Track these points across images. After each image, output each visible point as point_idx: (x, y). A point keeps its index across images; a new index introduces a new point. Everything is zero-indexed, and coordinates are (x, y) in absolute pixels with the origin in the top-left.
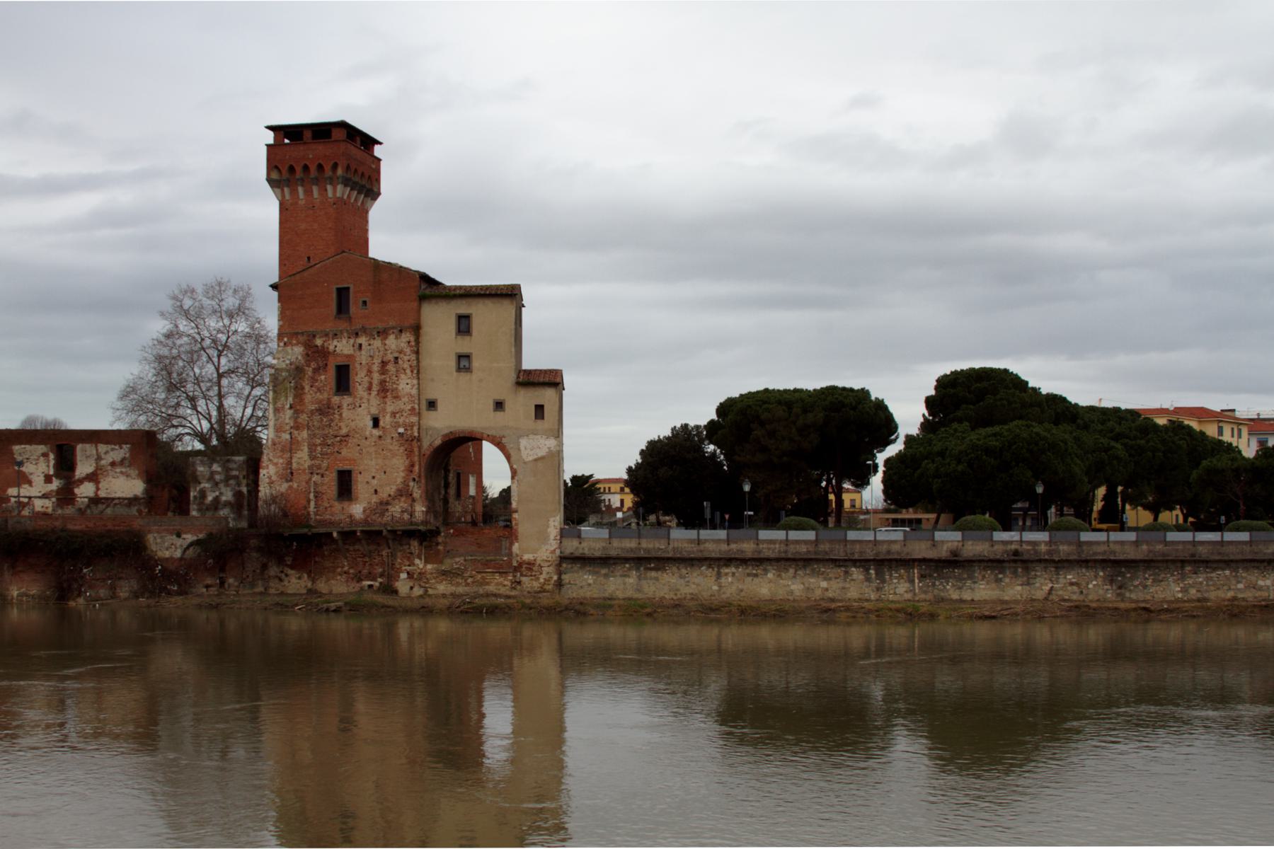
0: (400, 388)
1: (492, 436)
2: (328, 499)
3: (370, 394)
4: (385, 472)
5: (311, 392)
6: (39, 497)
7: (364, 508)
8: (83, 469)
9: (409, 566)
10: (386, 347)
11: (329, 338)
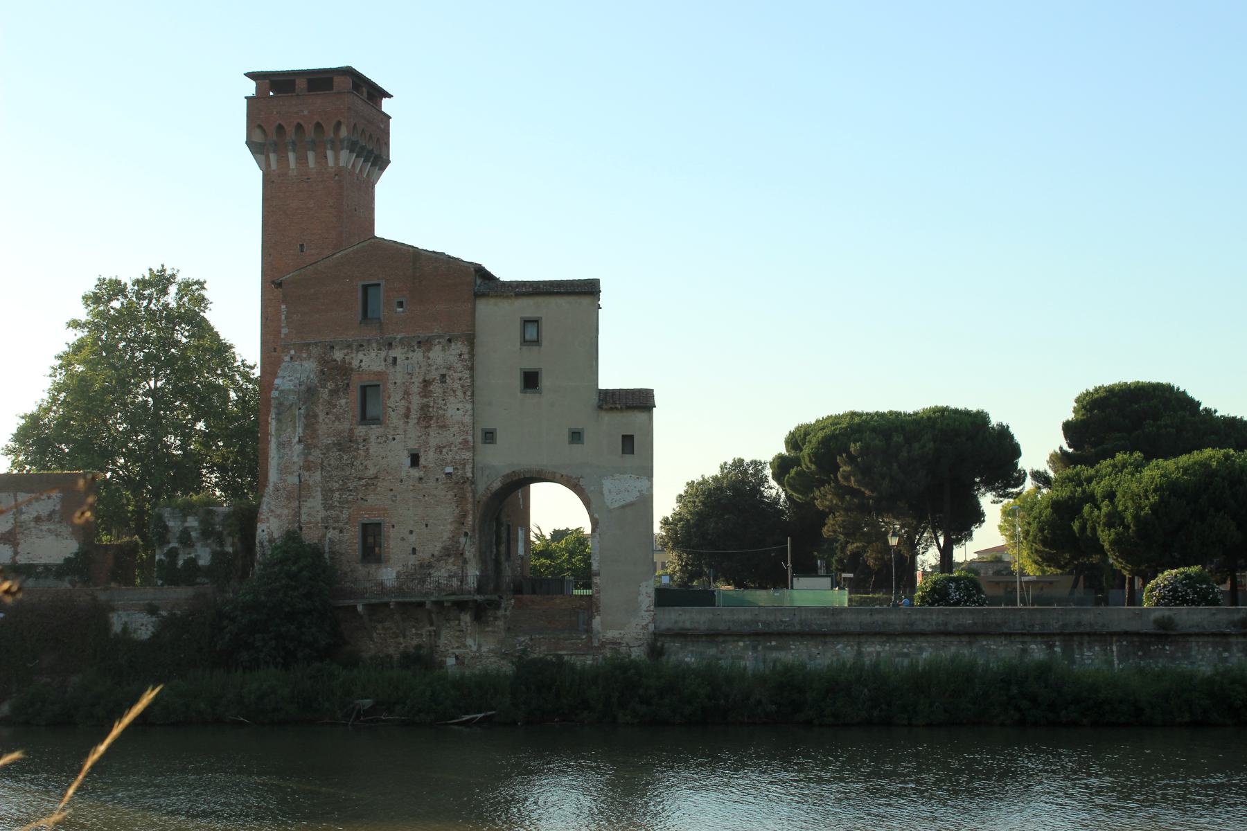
0: (449, 413)
1: (567, 476)
2: (348, 562)
3: (408, 422)
4: (427, 525)
5: (327, 421)
7: (398, 573)
9: (458, 648)
10: (430, 362)
11: (352, 350)
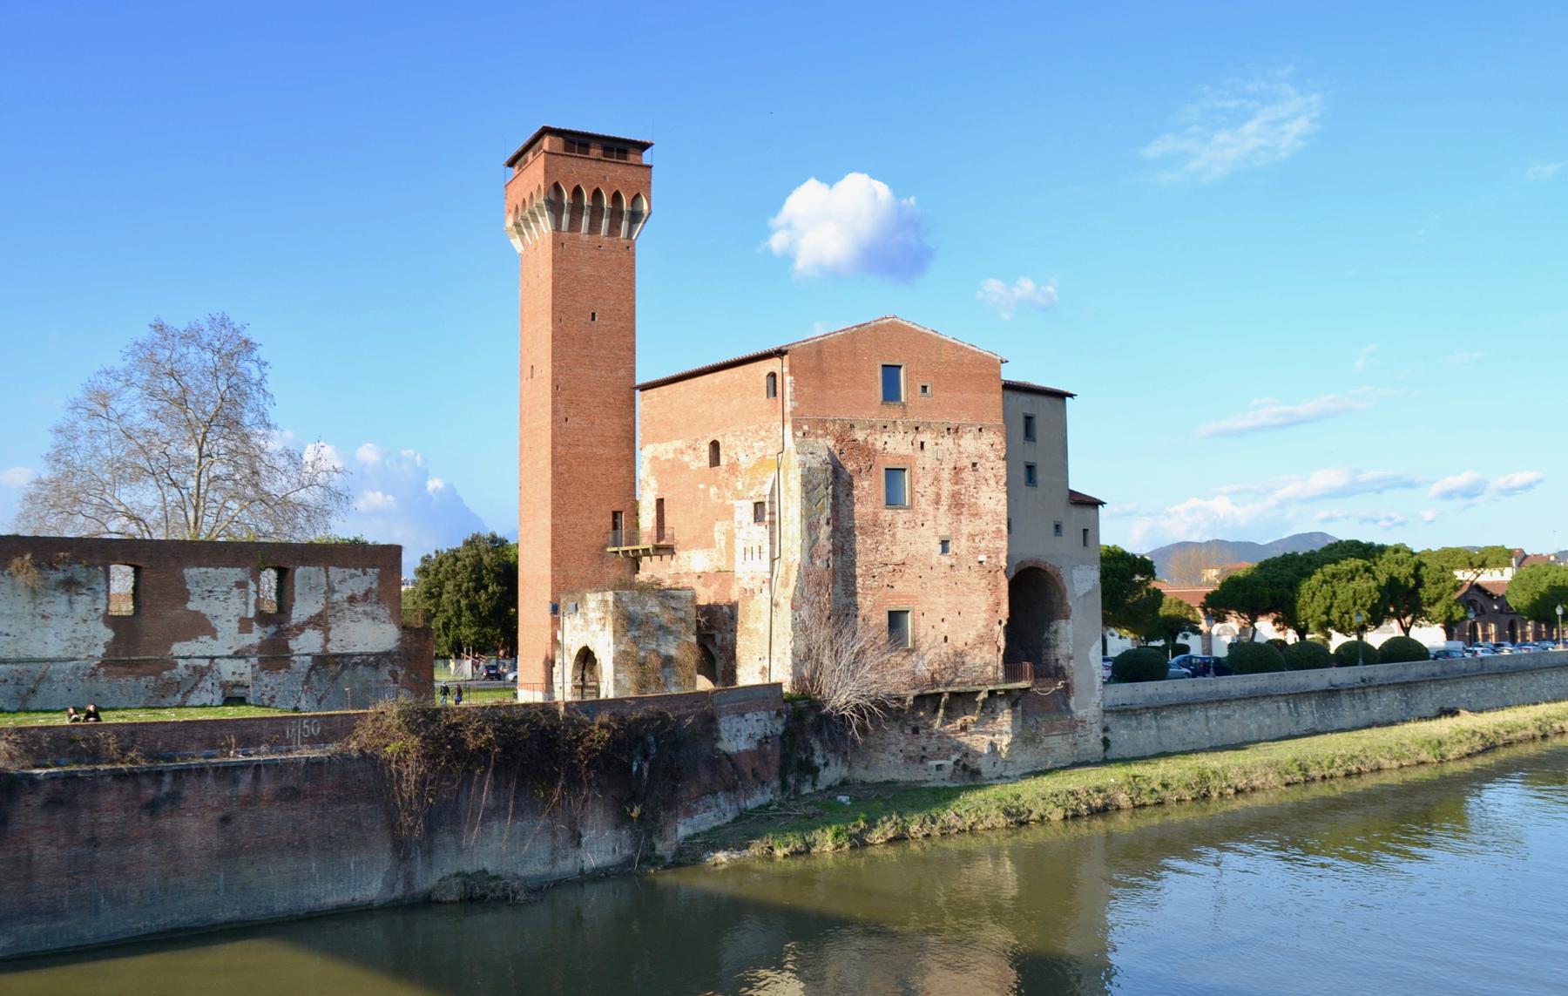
0: (980, 502)
6: (229, 657)
8: (302, 609)
10: (961, 449)
